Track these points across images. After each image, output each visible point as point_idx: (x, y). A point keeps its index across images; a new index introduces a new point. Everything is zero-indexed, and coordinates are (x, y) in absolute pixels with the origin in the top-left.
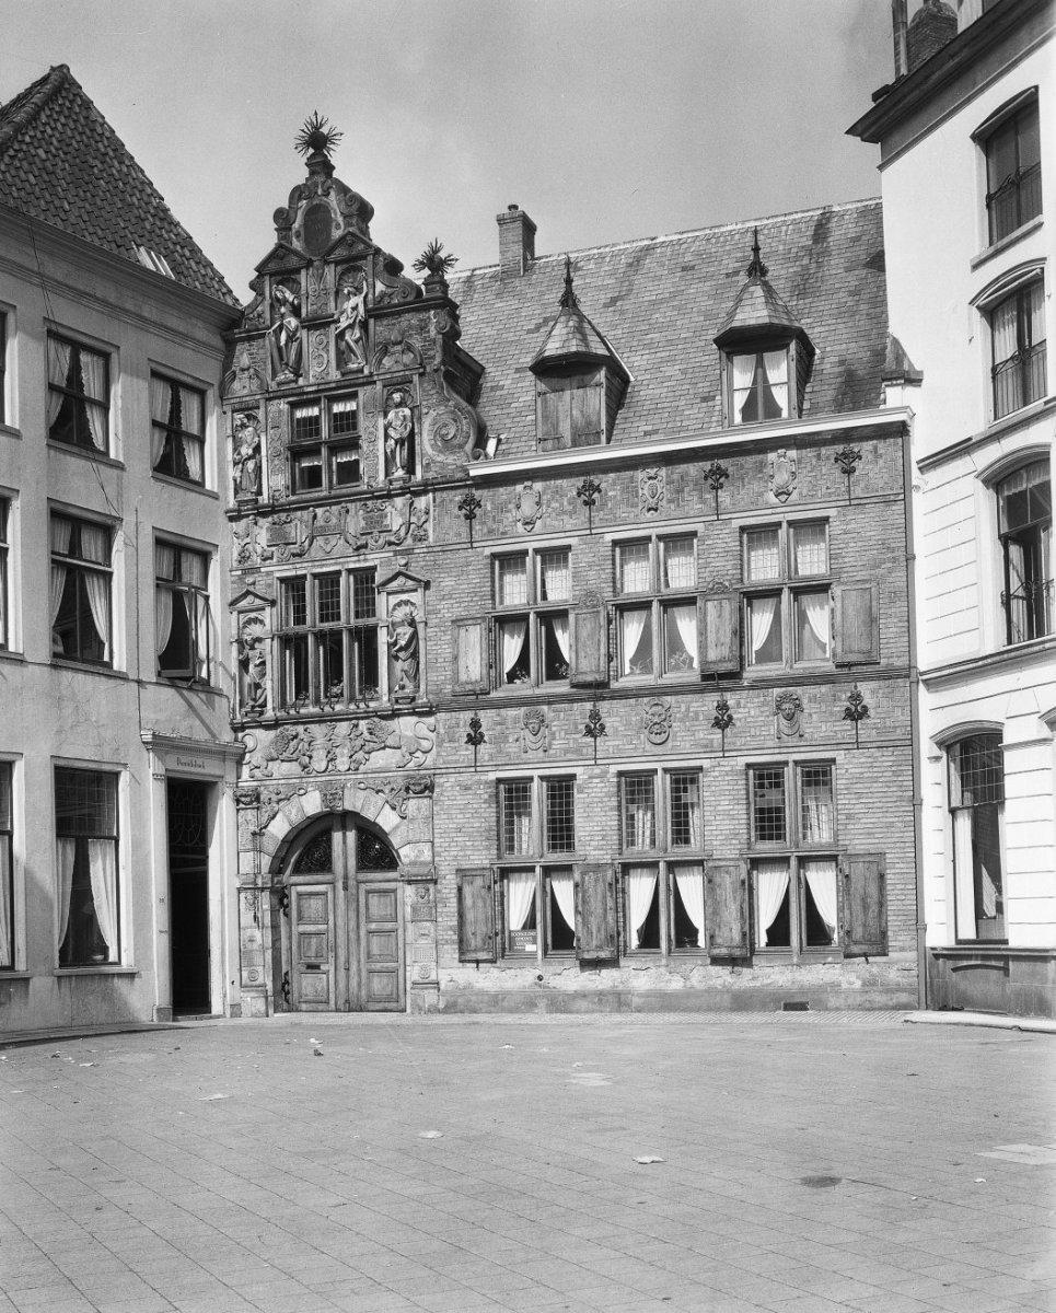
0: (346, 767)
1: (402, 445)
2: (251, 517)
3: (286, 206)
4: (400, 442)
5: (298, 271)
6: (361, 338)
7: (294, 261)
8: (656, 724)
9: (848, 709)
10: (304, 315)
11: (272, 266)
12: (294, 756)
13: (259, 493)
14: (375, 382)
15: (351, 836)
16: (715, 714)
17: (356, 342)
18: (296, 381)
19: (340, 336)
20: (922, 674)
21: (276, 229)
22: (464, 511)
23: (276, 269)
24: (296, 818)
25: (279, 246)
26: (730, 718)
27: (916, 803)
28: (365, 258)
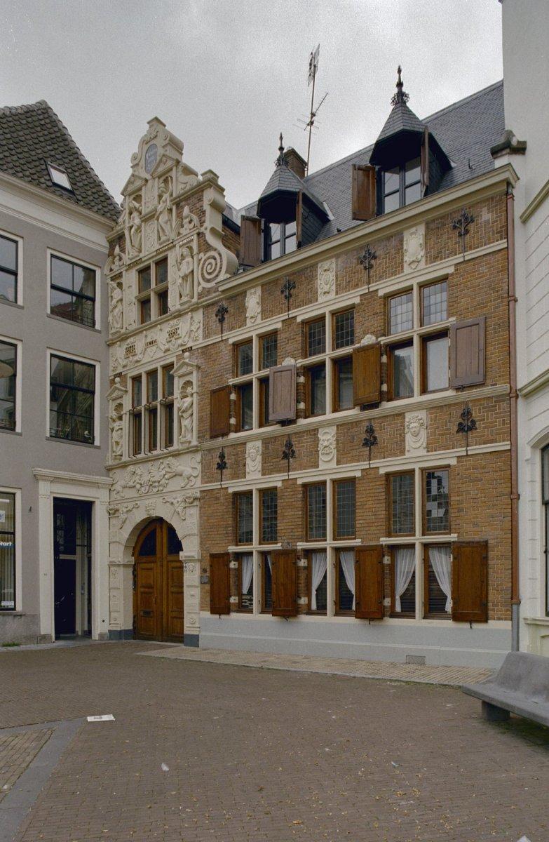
2: (118, 343)
5: (140, 189)
7: (138, 183)
9: (460, 424)
10: (143, 213)
11: (131, 189)
12: (133, 485)
16: (364, 436)
17: (166, 223)
18: (139, 256)
20: (521, 390)
21: (132, 167)
22: (218, 317)
23: (133, 192)
25: (133, 175)
26: (375, 438)
27: (514, 497)
28: (171, 169)
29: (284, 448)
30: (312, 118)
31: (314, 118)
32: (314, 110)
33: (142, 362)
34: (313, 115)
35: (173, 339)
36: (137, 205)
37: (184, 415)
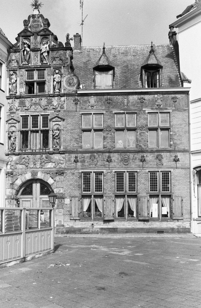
0: (39, 167)
1: (58, 83)
3: (27, 19)
4: (58, 82)
5: (30, 36)
6: (47, 55)
7: (28, 34)
8: (126, 160)
10: (31, 48)
12: (24, 163)
13: (16, 93)
14: (51, 67)
15: (38, 185)
17: (46, 56)
18: (28, 65)
19: (42, 54)
24: (24, 180)
29: (107, 158)
30: (82, 22)
31: (83, 22)
32: (83, 20)
33: (29, 111)
34: (83, 21)
35: (50, 105)
36: (28, 43)
37: (56, 138)
